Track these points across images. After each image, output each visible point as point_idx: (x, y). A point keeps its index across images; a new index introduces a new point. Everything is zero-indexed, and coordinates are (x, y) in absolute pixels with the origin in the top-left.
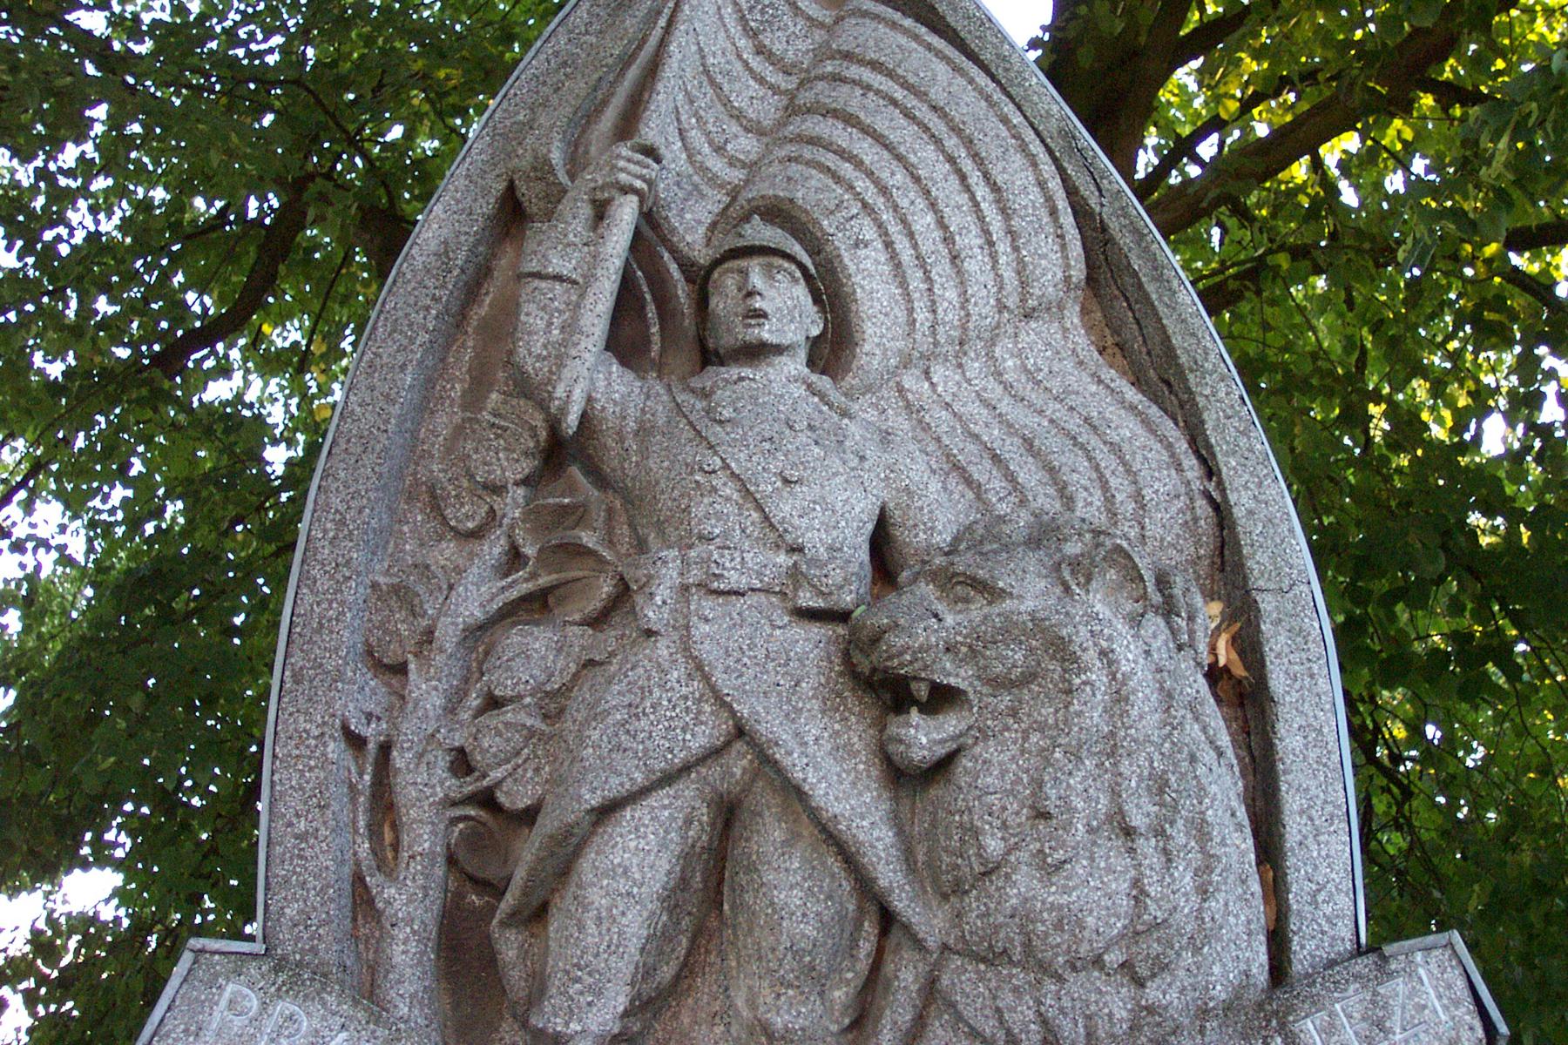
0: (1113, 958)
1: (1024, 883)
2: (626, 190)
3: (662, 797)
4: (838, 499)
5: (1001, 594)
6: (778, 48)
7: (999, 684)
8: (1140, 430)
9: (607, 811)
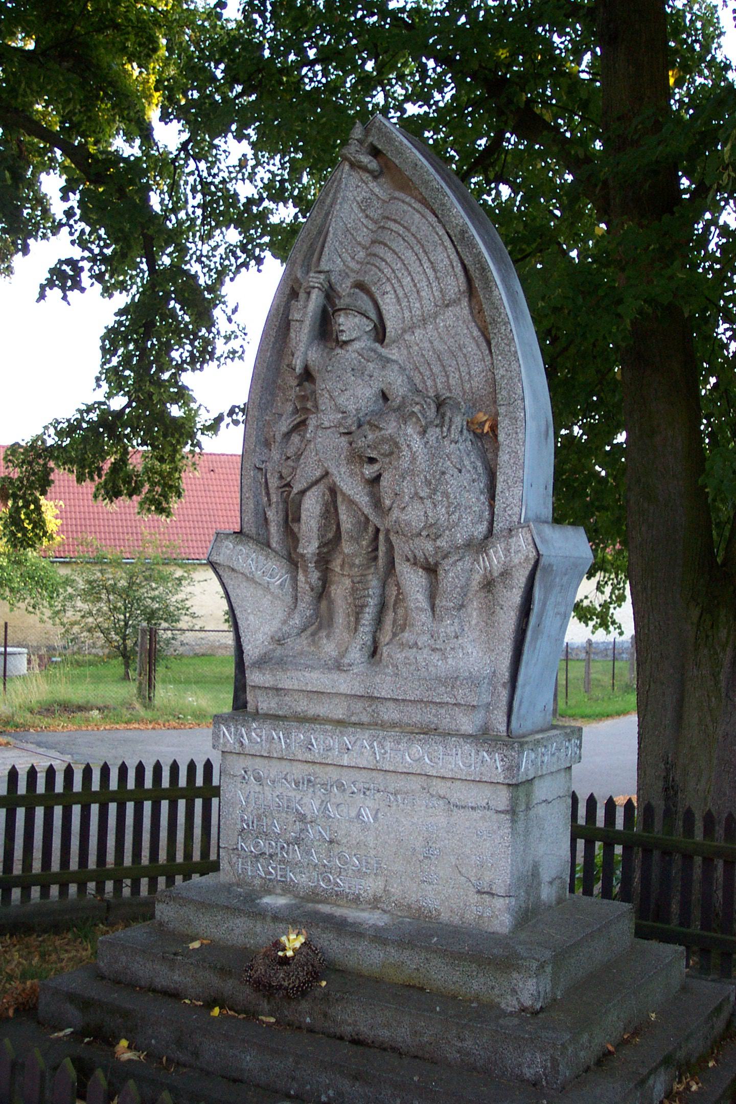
0: (424, 533)
1: (395, 513)
2: (314, 287)
3: (314, 489)
4: (359, 392)
5: (381, 429)
6: (371, 215)
7: (385, 455)
8: (475, 348)
9: (303, 492)
